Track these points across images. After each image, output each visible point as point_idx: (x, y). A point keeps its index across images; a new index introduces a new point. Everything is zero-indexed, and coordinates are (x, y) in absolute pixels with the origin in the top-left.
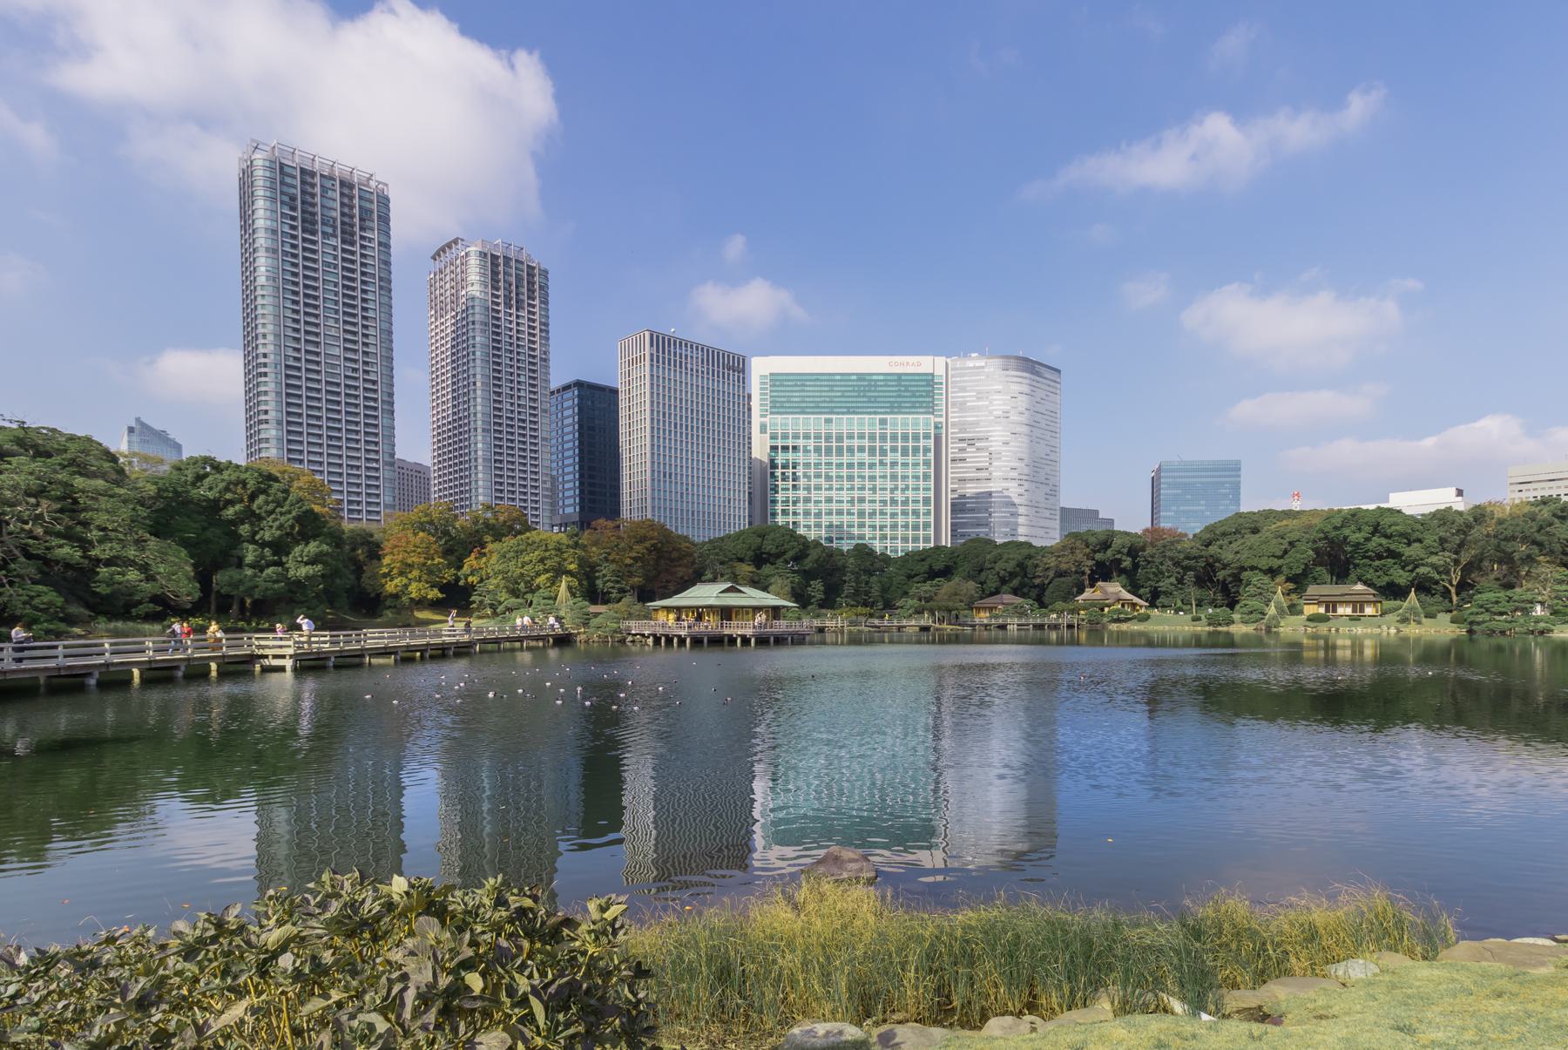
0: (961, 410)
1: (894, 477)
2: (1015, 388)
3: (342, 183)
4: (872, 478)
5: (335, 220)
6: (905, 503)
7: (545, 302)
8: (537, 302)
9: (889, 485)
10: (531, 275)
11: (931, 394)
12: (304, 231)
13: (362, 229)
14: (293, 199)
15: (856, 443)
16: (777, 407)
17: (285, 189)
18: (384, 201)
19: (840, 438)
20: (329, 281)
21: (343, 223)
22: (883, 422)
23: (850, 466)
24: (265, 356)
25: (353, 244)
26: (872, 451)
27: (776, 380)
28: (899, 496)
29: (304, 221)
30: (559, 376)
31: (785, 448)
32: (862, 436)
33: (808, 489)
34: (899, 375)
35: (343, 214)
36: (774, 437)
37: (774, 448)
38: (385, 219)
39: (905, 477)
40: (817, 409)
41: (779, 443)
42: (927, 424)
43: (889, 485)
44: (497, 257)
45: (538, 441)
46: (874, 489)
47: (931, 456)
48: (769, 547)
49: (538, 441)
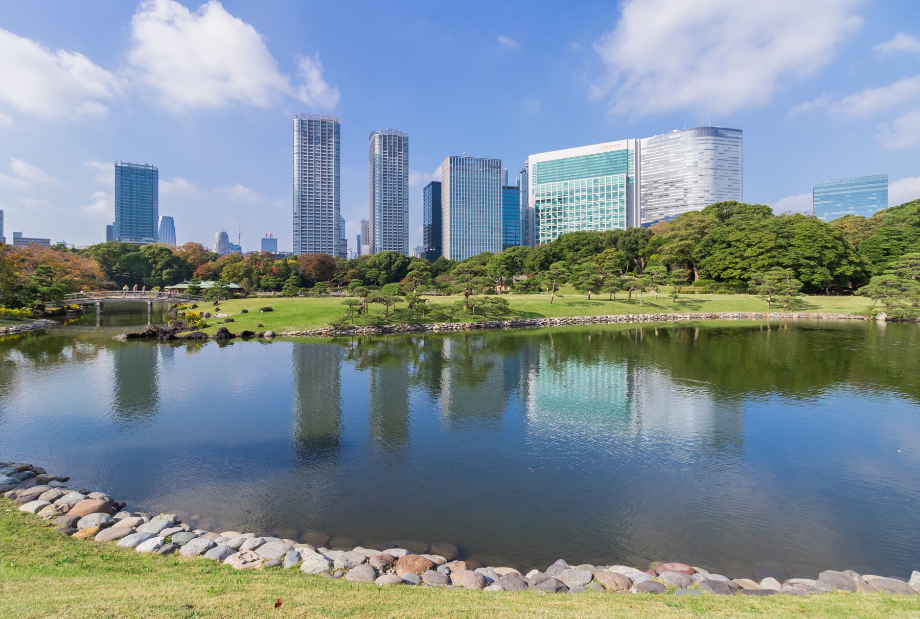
0: (666, 165)
1: (602, 211)
2: (702, 147)
7: (407, 151)
9: (600, 216)
15: (581, 194)
16: (540, 180)
19: (572, 193)
23: (578, 207)
26: (590, 198)
31: (543, 201)
32: (584, 191)
37: (538, 202)
40: (561, 178)
41: (540, 198)
46: (591, 219)
47: (624, 197)
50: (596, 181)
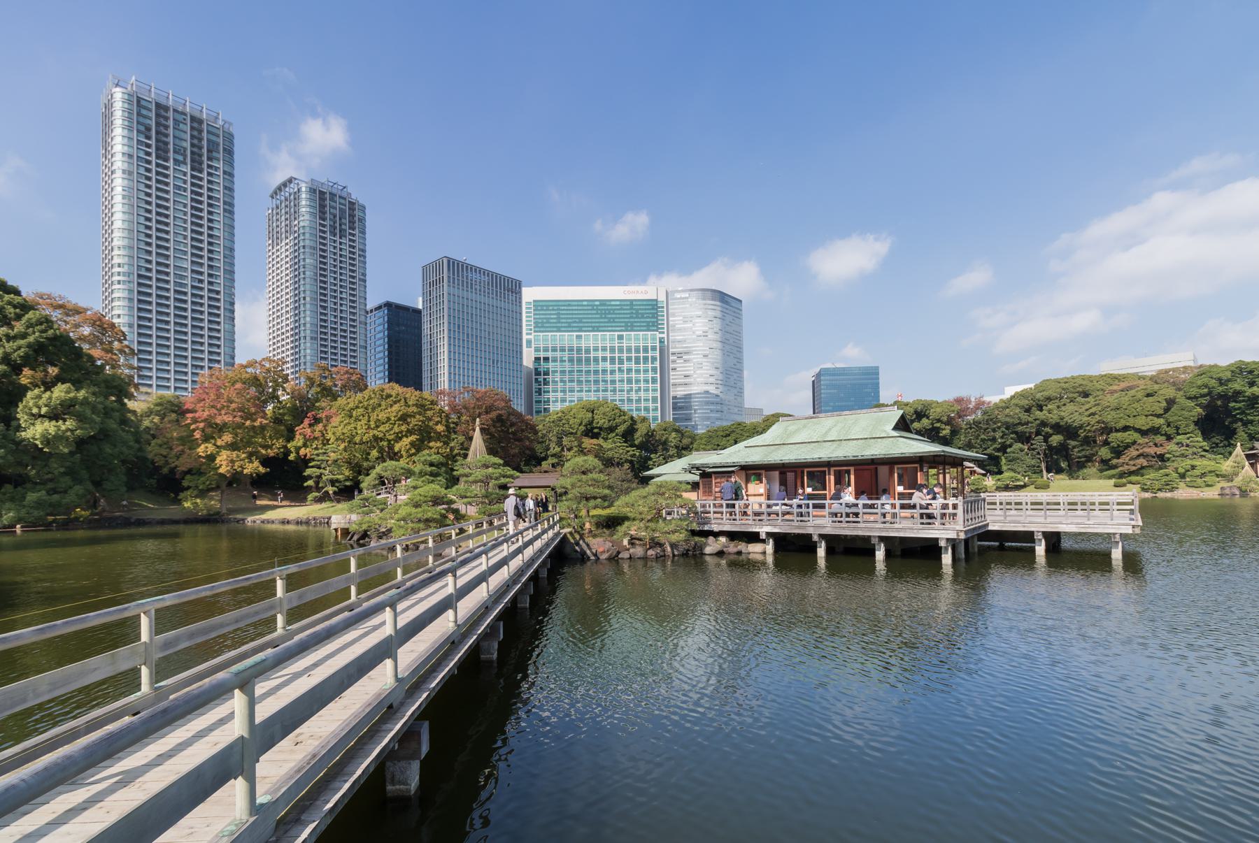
1: (629, 381)
2: (711, 313)
3: (193, 119)
4: (613, 382)
5: (185, 149)
6: (639, 401)
8: (356, 232)
10: (352, 209)
11: (655, 316)
12: (157, 157)
13: (209, 159)
14: (148, 129)
15: (600, 354)
16: (540, 326)
17: (141, 120)
18: (229, 138)
19: (588, 351)
21: (192, 153)
22: (620, 337)
23: (596, 372)
24: (119, 265)
25: (201, 171)
26: (613, 360)
27: (539, 305)
28: (634, 396)
29: (157, 149)
31: (546, 359)
33: (564, 391)
34: (631, 301)
35: (193, 145)
36: (537, 350)
38: (229, 152)
39: (638, 381)
40: (569, 328)
41: (542, 355)
42: (654, 339)
43: (626, 386)
44: (324, 193)
45: (357, 348)
47: (657, 364)
48: (601, 421)
49: (357, 348)
50: (620, 337)
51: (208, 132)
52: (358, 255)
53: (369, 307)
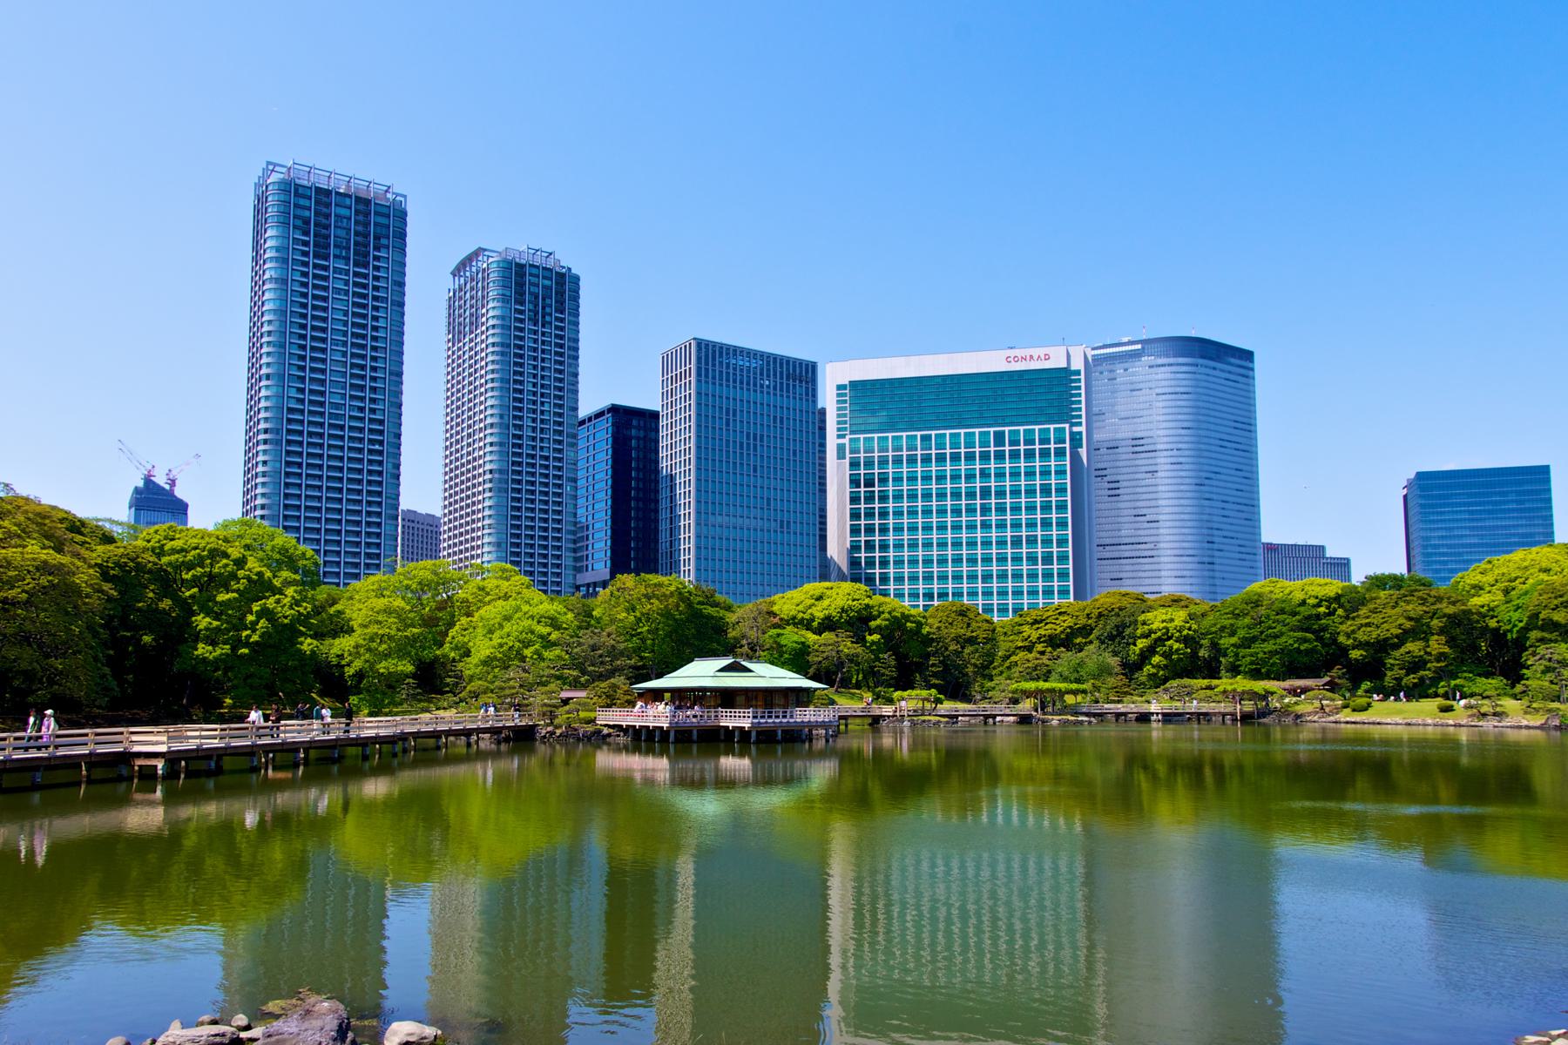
12: (315, 257)
14: (307, 222)
17: (300, 212)
18: (402, 216)
20: (339, 308)
25: (366, 266)
30: (590, 400)
36: (854, 464)
51: (376, 213)
52: (567, 351)
53: (583, 413)
